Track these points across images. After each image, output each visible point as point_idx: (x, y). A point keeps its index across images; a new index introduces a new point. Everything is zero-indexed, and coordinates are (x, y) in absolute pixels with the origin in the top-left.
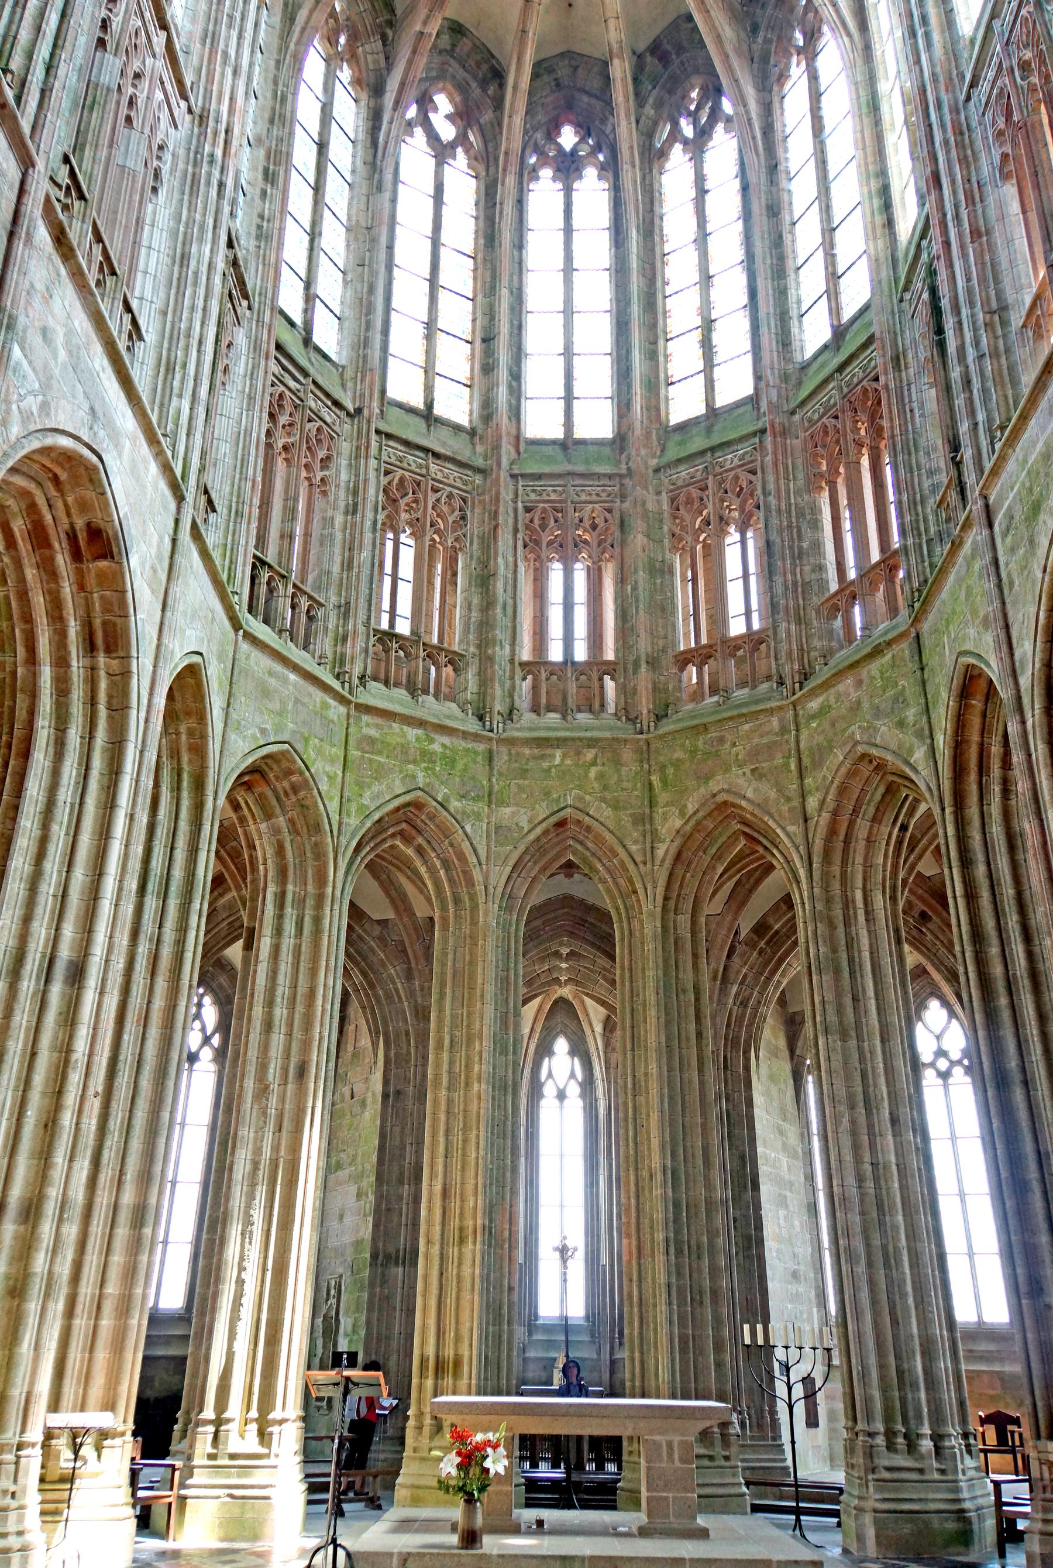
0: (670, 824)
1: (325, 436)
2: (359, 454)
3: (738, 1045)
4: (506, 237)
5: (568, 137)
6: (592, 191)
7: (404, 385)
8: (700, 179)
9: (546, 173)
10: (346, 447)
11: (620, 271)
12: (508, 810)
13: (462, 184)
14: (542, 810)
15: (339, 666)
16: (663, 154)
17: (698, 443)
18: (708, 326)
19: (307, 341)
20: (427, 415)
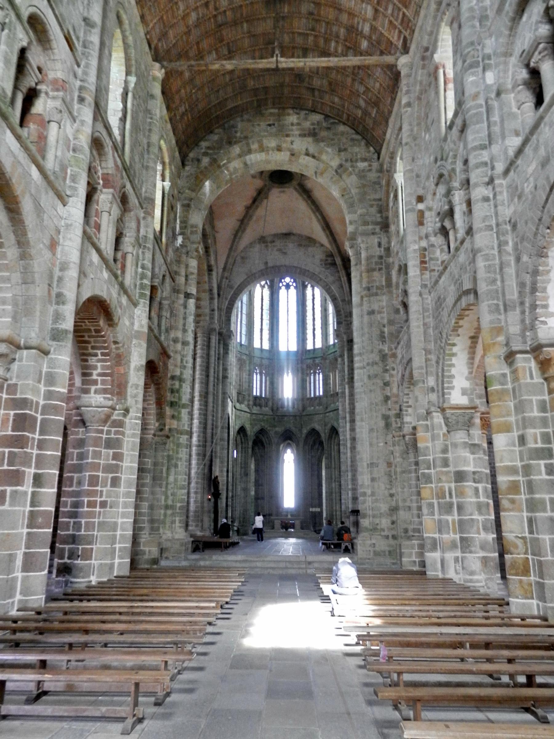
0: (305, 431)
1: (245, 361)
2: (250, 363)
3: (320, 461)
4: (275, 304)
5: (288, 280)
6: (293, 291)
7: (257, 344)
8: (313, 295)
9: (283, 288)
10: (248, 362)
11: (298, 312)
12: (277, 429)
13: (267, 292)
14: (283, 428)
15: (248, 406)
16: (306, 286)
17: (311, 356)
18: (314, 329)
19: (241, 345)
20: (261, 350)
